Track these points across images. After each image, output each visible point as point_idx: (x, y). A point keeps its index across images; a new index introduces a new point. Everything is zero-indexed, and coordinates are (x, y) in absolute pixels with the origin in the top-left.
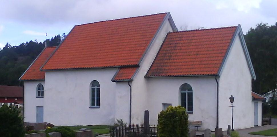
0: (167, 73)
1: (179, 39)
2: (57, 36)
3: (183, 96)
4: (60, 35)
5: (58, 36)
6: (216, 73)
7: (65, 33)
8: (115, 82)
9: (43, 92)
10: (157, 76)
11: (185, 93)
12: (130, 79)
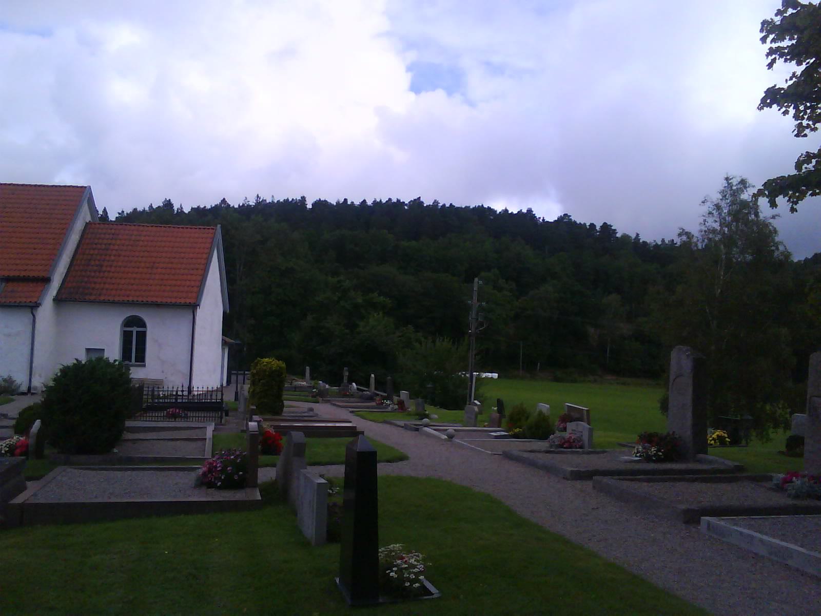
0: (100, 295)
1: (111, 236)
3: (126, 338)
6: (192, 301)
10: (80, 299)
12: (36, 302)
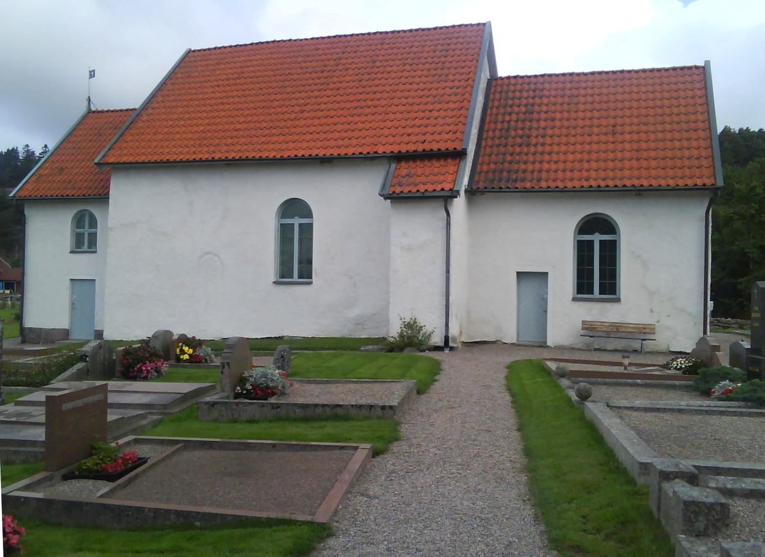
2: (12, 150)
3: (583, 251)
4: (17, 148)
5: (13, 149)
7: (29, 145)
8: (389, 200)
9: (93, 239)
11: (593, 241)
12: (451, 190)
